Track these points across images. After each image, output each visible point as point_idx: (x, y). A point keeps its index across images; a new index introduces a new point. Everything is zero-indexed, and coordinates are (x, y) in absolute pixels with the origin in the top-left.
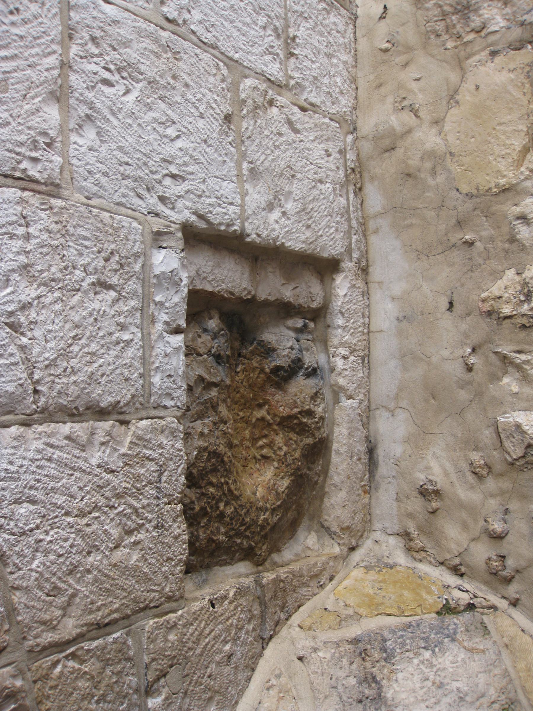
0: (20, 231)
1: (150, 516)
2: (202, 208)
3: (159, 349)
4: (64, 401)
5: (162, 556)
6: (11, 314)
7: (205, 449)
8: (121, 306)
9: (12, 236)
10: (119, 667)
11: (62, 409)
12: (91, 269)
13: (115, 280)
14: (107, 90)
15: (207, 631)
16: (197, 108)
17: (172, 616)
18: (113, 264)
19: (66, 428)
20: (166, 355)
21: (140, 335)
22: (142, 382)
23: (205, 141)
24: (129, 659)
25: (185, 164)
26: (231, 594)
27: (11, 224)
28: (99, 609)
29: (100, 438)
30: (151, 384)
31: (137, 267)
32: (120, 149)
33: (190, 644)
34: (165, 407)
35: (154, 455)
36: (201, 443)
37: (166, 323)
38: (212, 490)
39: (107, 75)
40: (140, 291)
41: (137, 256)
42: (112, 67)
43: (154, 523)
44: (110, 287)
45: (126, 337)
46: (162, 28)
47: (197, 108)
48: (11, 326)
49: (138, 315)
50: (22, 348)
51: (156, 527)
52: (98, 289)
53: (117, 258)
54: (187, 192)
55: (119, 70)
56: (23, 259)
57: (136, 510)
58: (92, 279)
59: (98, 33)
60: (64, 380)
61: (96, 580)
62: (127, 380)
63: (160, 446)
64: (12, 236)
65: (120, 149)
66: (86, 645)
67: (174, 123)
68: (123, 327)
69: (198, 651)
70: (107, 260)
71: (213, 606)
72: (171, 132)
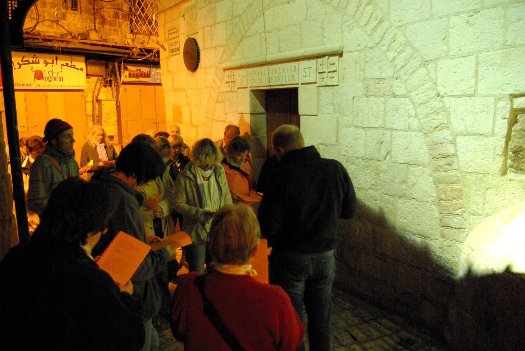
0: (465, 104)
1: (491, 156)
2: (516, 89)
3: (497, 123)
4: (472, 132)
5: (494, 165)
6: (462, 118)
7: (517, 146)
8: (488, 115)
9: (463, 105)
10: (480, 182)
11: (472, 133)
12: (480, 108)
13: (486, 110)
14: (488, 71)
15: (506, 185)
16: (517, 64)
17: (495, 178)
18: (486, 107)
19: (472, 137)
20: (499, 124)
21: (492, 120)
22: (491, 129)
23: (519, 72)
24: (483, 181)
25: (511, 80)
26: (518, 180)
27: (463, 103)
28: (476, 169)
29: (480, 139)
30: (494, 130)
31: (493, 106)
32: (490, 82)
33: (499, 185)
34: (498, 135)
35: (493, 144)
36: (517, 144)
37: (500, 117)
38: (520, 156)
39: (487, 68)
40: (493, 110)
41: (492, 104)
42: (488, 66)
43: (492, 158)
44: (485, 111)
45: (488, 120)
46: (505, 49)
47: (517, 64)
48: (462, 120)
49: (493, 116)
50: (464, 123)
51: (493, 159)
52: (482, 112)
53: (487, 105)
54: (511, 86)
55: (491, 65)
56: (465, 109)
57: (487, 154)
58: (481, 110)
59: (484, 60)
60: (472, 129)
61: (476, 164)
62: (487, 129)
63: (495, 143)
64: (463, 105)
65: (490, 82)
66: (473, 175)
67: (508, 71)
68: (487, 119)
69: (502, 187)
70: (484, 106)
71: (510, 181)
72: (506, 74)
